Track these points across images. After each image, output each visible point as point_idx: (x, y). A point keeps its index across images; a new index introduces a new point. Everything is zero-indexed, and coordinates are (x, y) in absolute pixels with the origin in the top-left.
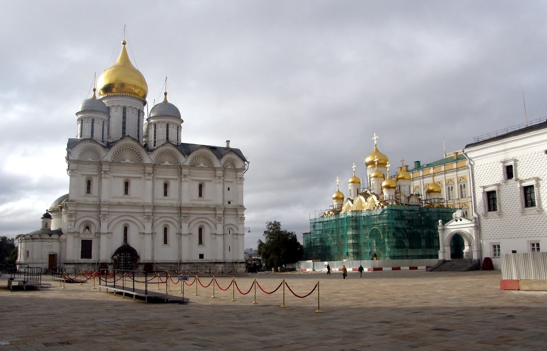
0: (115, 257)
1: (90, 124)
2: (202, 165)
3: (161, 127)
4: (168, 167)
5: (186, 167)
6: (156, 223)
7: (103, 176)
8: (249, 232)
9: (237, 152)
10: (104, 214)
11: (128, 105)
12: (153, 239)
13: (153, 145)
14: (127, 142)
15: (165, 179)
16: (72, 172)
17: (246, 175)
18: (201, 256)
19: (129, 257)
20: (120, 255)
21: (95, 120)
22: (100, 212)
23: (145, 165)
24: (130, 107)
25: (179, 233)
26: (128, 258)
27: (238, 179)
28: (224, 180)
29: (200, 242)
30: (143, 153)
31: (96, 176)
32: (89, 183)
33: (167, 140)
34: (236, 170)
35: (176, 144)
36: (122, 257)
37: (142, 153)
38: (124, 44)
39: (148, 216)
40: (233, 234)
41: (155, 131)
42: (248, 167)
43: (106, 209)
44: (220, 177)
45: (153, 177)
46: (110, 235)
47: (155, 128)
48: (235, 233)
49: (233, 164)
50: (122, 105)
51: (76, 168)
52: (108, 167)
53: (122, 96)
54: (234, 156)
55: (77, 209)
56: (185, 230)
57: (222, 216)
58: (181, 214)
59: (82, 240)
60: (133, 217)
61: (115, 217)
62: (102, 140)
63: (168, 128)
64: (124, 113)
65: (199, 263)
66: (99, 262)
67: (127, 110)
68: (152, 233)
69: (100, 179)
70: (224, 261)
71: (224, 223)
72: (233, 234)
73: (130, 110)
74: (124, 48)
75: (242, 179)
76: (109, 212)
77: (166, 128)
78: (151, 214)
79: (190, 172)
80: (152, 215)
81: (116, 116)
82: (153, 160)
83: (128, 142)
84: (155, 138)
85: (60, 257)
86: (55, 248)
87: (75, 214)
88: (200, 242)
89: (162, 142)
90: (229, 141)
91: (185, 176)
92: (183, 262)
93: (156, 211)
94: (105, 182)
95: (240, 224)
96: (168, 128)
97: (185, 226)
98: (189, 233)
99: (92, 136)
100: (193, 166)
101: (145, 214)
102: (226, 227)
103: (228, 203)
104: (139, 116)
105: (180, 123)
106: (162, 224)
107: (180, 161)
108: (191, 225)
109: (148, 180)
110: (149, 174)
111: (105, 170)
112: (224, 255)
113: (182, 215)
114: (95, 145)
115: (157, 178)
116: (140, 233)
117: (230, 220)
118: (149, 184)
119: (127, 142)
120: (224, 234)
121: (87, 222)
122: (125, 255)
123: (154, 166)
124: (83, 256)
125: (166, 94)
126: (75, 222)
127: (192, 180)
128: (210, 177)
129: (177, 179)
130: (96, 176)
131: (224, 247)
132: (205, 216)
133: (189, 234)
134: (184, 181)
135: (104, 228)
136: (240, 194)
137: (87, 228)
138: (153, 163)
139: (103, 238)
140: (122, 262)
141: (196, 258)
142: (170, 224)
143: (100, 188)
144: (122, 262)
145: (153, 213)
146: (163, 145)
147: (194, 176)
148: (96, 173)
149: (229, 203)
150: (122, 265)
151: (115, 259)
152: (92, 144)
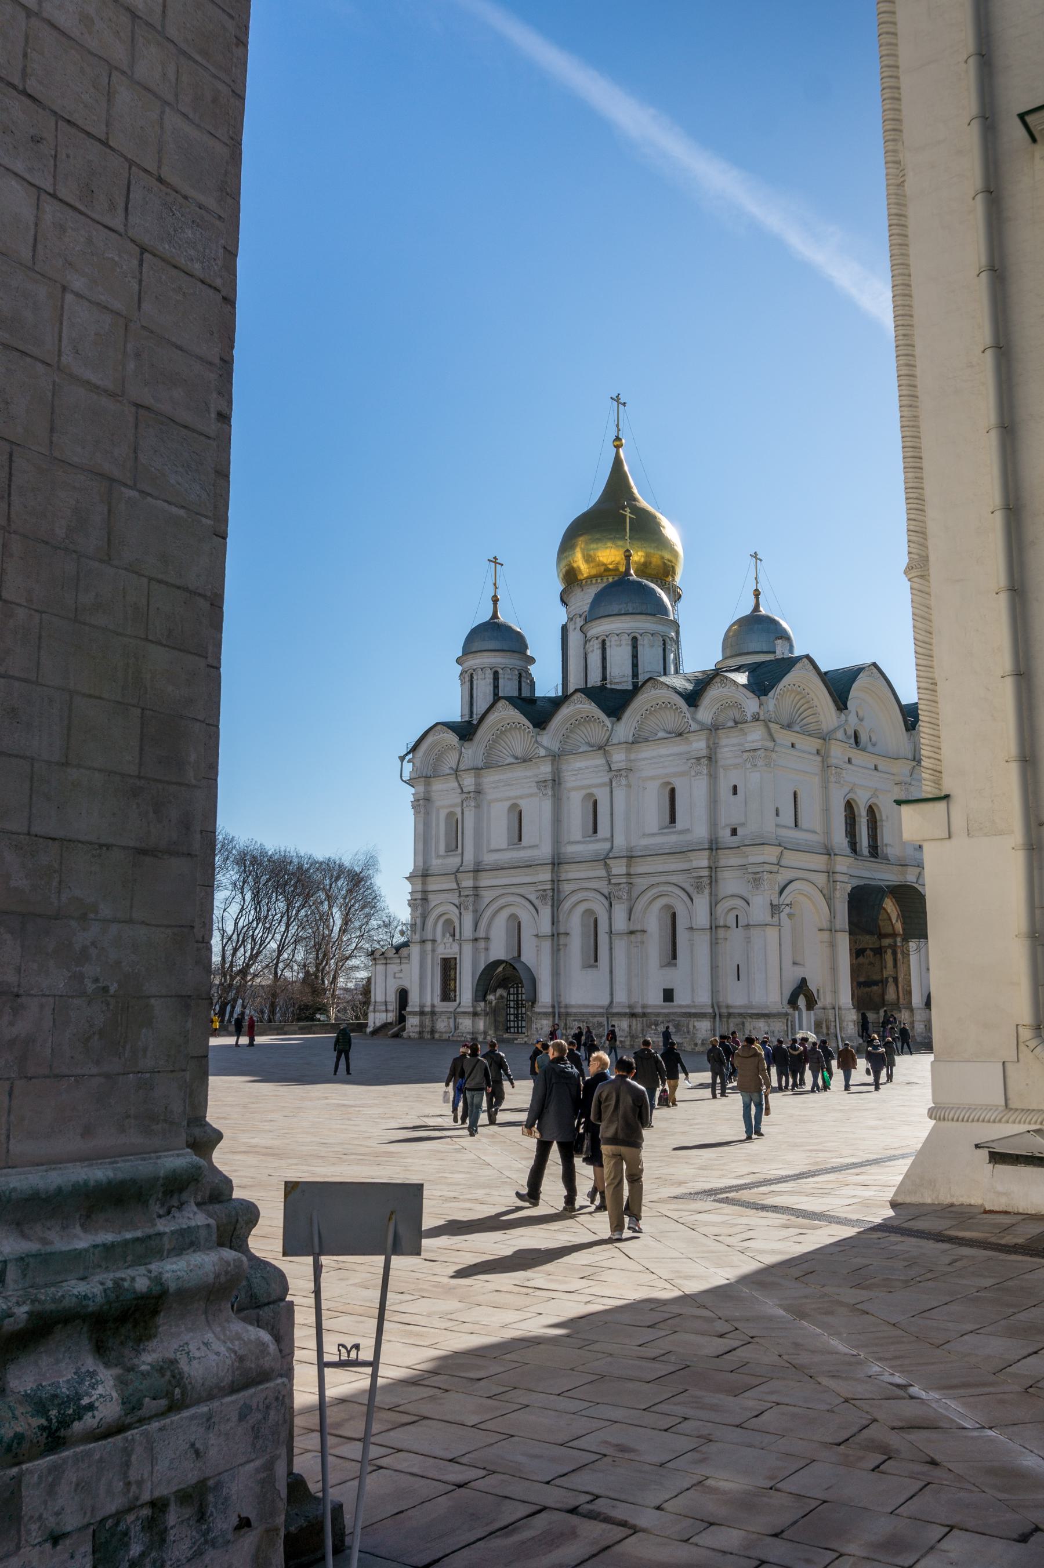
0: (491, 997)
6: (567, 905)
18: (668, 995)
20: (509, 994)
26: (522, 1000)
35: (630, 687)
36: (512, 997)
39: (544, 890)
44: (698, 759)
46: (482, 944)
57: (705, 873)
58: (610, 880)
65: (658, 1015)
66: (459, 1010)
68: (553, 935)
69: (463, 813)
70: (711, 1011)
71: (711, 894)
78: (549, 887)
87: (425, 899)
92: (615, 1010)
98: (632, 928)
103: (728, 832)
108: (640, 906)
112: (714, 992)
113: (613, 881)
118: (547, 805)
122: (518, 994)
131: (714, 968)
133: (632, 933)
140: (512, 1010)
141: (654, 999)
144: (512, 1012)
149: (734, 832)
150: (512, 1018)
151: (491, 1003)
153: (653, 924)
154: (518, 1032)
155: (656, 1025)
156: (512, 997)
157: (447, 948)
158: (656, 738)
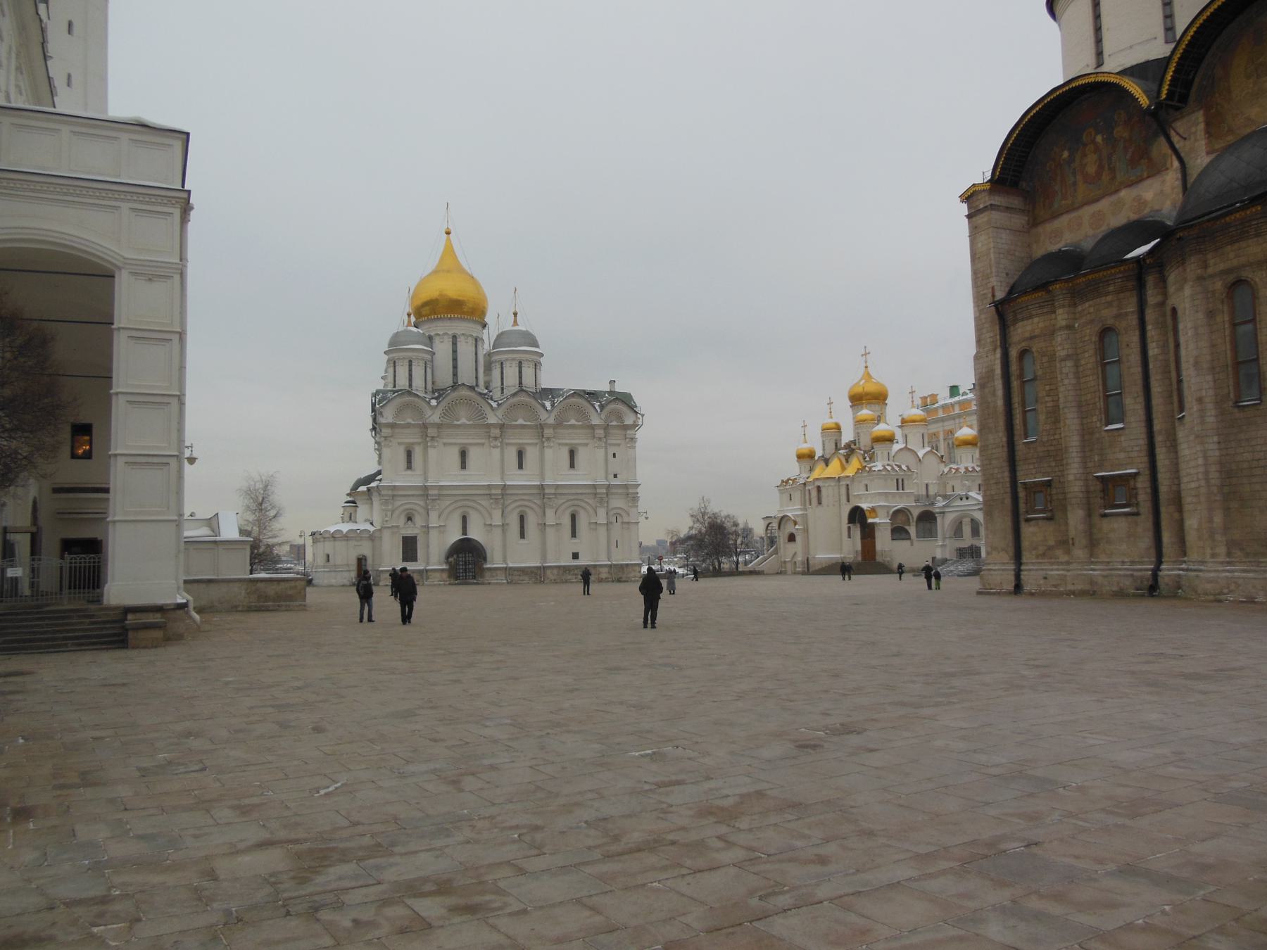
0: (451, 559)
1: (408, 366)
2: (573, 422)
4: (523, 426)
5: (550, 426)
7: (429, 444)
8: (647, 518)
9: (626, 400)
11: (458, 332)
12: (504, 532)
13: (499, 393)
15: (519, 444)
16: (385, 440)
17: (640, 434)
18: (576, 556)
19: (470, 559)
20: (458, 557)
21: (413, 361)
22: (427, 497)
24: (463, 334)
25: (541, 524)
27: (627, 440)
28: (606, 443)
29: (574, 534)
31: (419, 444)
32: (409, 454)
34: (626, 428)
36: (460, 559)
37: (484, 408)
38: (448, 233)
40: (623, 523)
41: (502, 373)
43: (436, 492)
44: (600, 438)
45: (501, 443)
47: (502, 368)
48: (625, 521)
49: (620, 417)
50: (450, 333)
51: (390, 435)
52: (436, 430)
53: (450, 319)
54: (620, 407)
55: (395, 493)
56: (550, 518)
57: (605, 496)
59: (403, 537)
60: (474, 501)
61: (449, 503)
62: (423, 389)
63: (520, 368)
64: (454, 344)
67: (458, 340)
71: (607, 506)
72: (623, 523)
73: (462, 338)
74: (449, 240)
75: (633, 439)
76: (439, 495)
77: (517, 369)
79: (555, 433)
80: (502, 498)
81: (442, 349)
82: (501, 417)
83: (463, 393)
84: (502, 384)
85: (373, 561)
86: (365, 549)
88: (574, 534)
89: (514, 390)
90: (614, 381)
91: (548, 439)
93: (508, 492)
94: (431, 452)
95: (631, 507)
96: (520, 368)
97: (550, 513)
99: (410, 385)
100: (559, 425)
101: (493, 497)
102: (612, 513)
103: (613, 476)
104: (476, 347)
105: (538, 358)
106: (518, 510)
107: (541, 417)
108: (559, 512)
109: (494, 447)
110: (496, 438)
111: (433, 435)
113: (546, 496)
114: (416, 399)
115: (507, 444)
116: (485, 524)
117: (617, 502)
118: (496, 452)
120: (608, 524)
121: (407, 512)
122: (465, 557)
123: (502, 427)
124: (405, 559)
125: (515, 314)
126: (393, 512)
127: (560, 444)
128: (587, 439)
129: (537, 444)
130: (419, 444)
132: (580, 497)
135: (434, 521)
136: (631, 463)
137: (409, 519)
138: (500, 422)
139: (433, 535)
140: (461, 567)
142: (527, 510)
143: (425, 461)
144: (461, 567)
145: (503, 495)
146: (514, 395)
147: (563, 439)
148: (419, 440)
150: (461, 571)
153: (567, 521)
154: (466, 579)
155: (570, 571)
156: (460, 559)
157: (410, 531)
158: (569, 423)
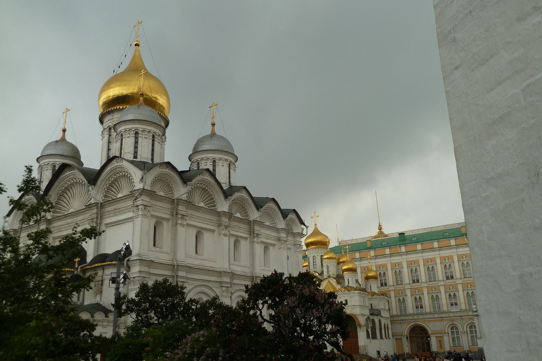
3: (223, 166)
10: (182, 282)
14: (204, 177)
16: (145, 209)
23: (219, 214)
30: (219, 197)
31: (168, 220)
33: (229, 185)
39: (227, 287)
42: (307, 232)
119: (204, 177)
128: (274, 240)
129: (246, 238)
130: (168, 220)
134: (257, 242)
143: (174, 239)
148: (168, 217)
152: (168, 171)
